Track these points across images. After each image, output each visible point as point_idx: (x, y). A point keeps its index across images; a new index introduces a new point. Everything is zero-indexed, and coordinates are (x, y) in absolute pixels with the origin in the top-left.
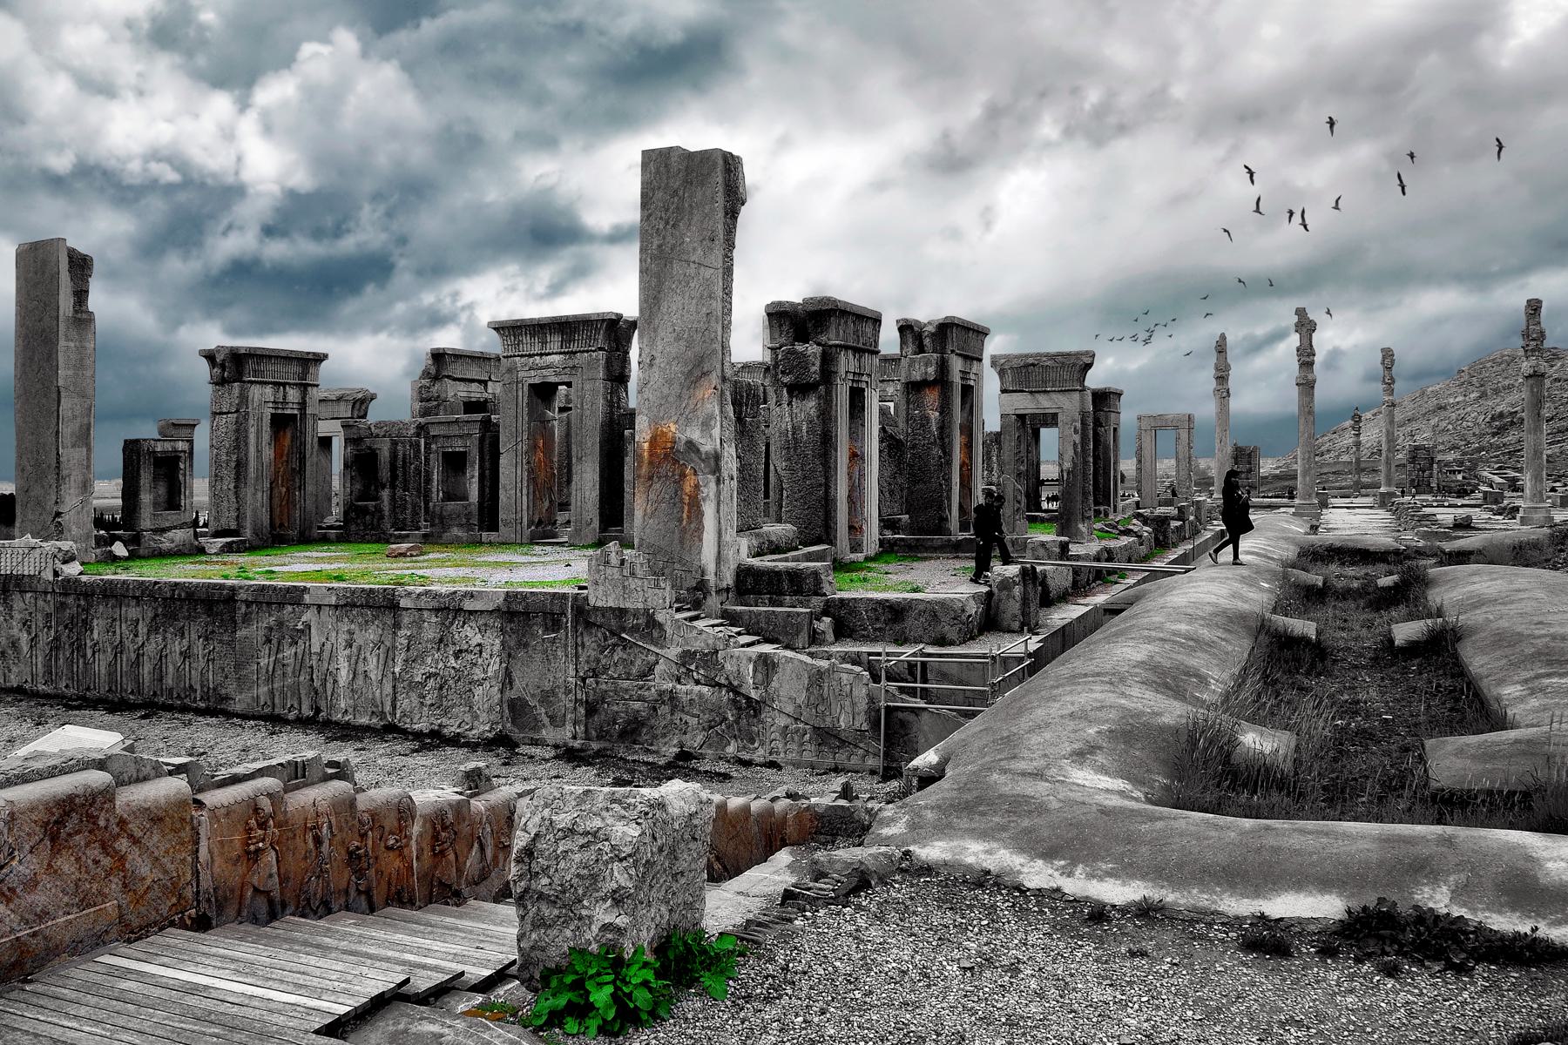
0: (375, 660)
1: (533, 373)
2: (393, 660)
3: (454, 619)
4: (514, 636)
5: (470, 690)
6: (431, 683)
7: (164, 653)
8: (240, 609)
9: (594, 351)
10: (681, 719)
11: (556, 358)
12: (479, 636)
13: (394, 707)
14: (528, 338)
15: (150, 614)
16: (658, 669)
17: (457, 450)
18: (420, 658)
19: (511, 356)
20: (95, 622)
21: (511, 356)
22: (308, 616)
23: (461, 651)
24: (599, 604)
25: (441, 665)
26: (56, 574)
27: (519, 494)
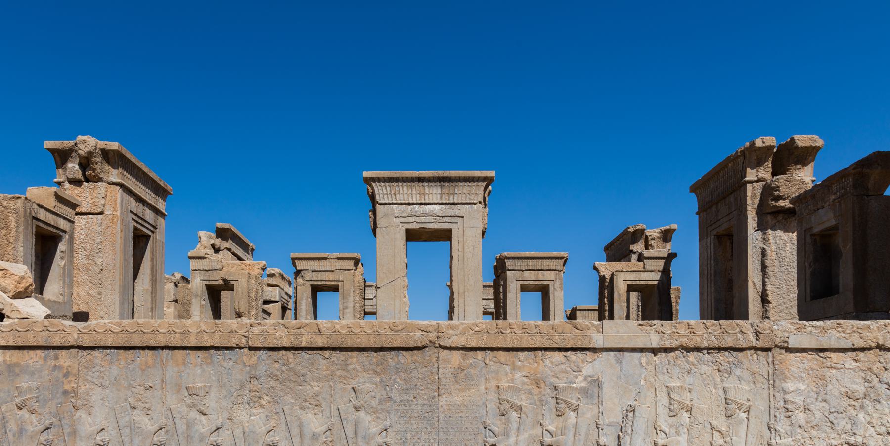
17: (328, 283)
19: (390, 204)
21: (390, 204)
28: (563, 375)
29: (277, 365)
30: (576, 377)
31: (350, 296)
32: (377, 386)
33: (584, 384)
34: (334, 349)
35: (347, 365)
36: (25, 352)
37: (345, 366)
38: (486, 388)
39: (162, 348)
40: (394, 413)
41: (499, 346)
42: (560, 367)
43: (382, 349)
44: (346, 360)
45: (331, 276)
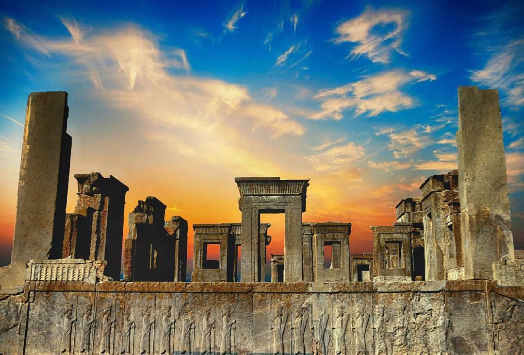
0: (361, 322)
1: (262, 204)
2: (373, 322)
3: (413, 296)
4: (453, 304)
5: (426, 334)
6: (399, 333)
7: (193, 326)
8: (256, 297)
9: (297, 195)
11: (276, 197)
15: (181, 303)
17: (214, 241)
18: (391, 319)
19: (248, 195)
20: (132, 309)
21: (248, 195)
22: (310, 299)
23: (418, 314)
26: (97, 280)
27: (253, 265)
29: (196, 299)
30: (303, 303)
33: (305, 306)
35: (220, 299)
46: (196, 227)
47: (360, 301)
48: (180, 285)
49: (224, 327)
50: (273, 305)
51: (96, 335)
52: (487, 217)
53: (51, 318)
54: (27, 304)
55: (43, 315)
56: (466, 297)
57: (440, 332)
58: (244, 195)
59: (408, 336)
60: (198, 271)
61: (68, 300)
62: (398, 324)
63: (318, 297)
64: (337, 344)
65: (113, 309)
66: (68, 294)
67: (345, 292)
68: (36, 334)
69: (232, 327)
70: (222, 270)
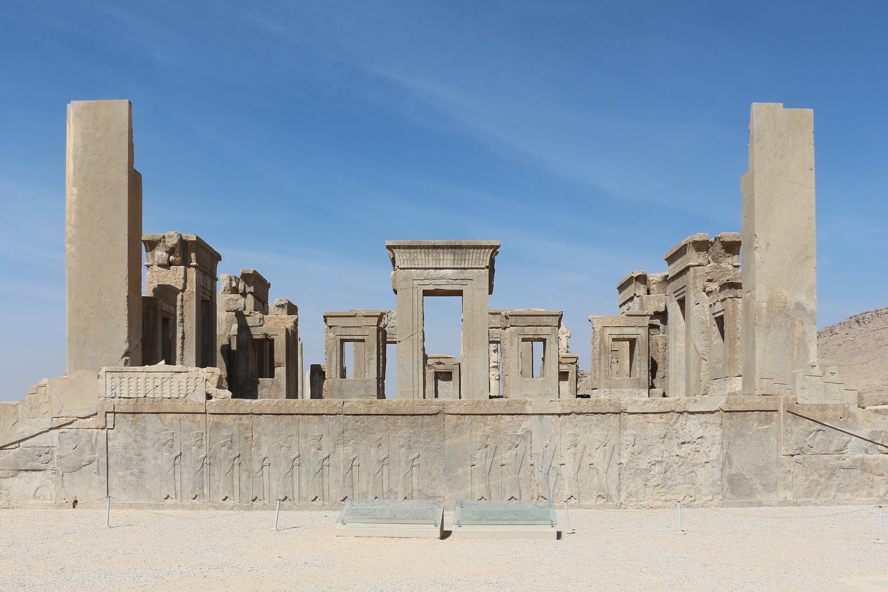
1: (427, 282)
6: (657, 469)
7: (356, 463)
8: (449, 421)
9: (484, 269)
10: (869, 478)
12: (701, 430)
13: (619, 491)
14: (423, 255)
16: (850, 445)
17: (355, 337)
22: (529, 423)
24: (806, 402)
25: (666, 454)
26: (209, 397)
27: (416, 373)
28: (511, 428)
29: (358, 424)
30: (518, 429)
31: (374, 349)
32: (412, 434)
33: (522, 433)
34: (389, 415)
36: (225, 415)
37: (395, 424)
38: (470, 436)
39: (297, 414)
40: (421, 449)
41: (477, 413)
42: (509, 424)
43: (414, 415)
44: (395, 421)
45: (358, 332)
46: (328, 316)
47: (602, 425)
48: (334, 403)
49: (403, 463)
50: (474, 433)
51: (212, 476)
52: (782, 305)
53: (142, 451)
54: (104, 431)
55: (130, 448)
56: (752, 419)
57: (713, 467)
58: (401, 269)
59: (668, 473)
60: (333, 381)
61: (166, 425)
62: (655, 457)
63: (541, 421)
64: (566, 485)
65: (236, 439)
66: (165, 417)
67: (579, 414)
68: (122, 474)
69: (414, 463)
70: (369, 380)
